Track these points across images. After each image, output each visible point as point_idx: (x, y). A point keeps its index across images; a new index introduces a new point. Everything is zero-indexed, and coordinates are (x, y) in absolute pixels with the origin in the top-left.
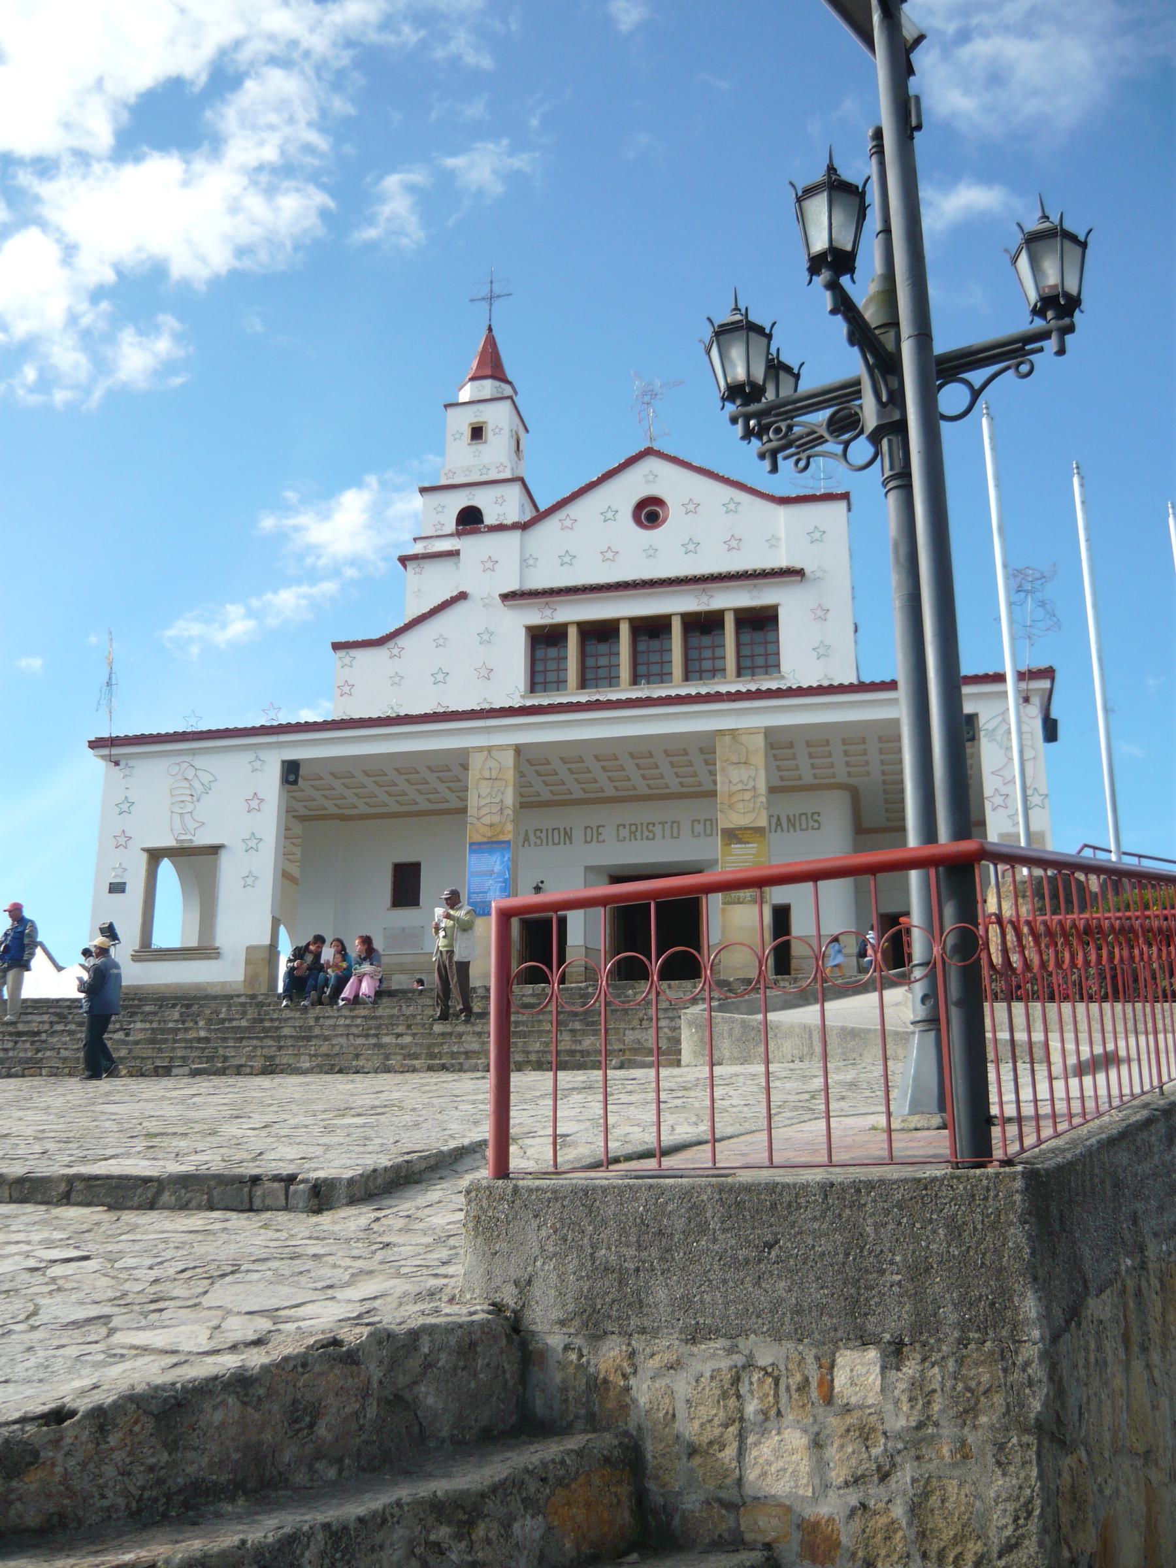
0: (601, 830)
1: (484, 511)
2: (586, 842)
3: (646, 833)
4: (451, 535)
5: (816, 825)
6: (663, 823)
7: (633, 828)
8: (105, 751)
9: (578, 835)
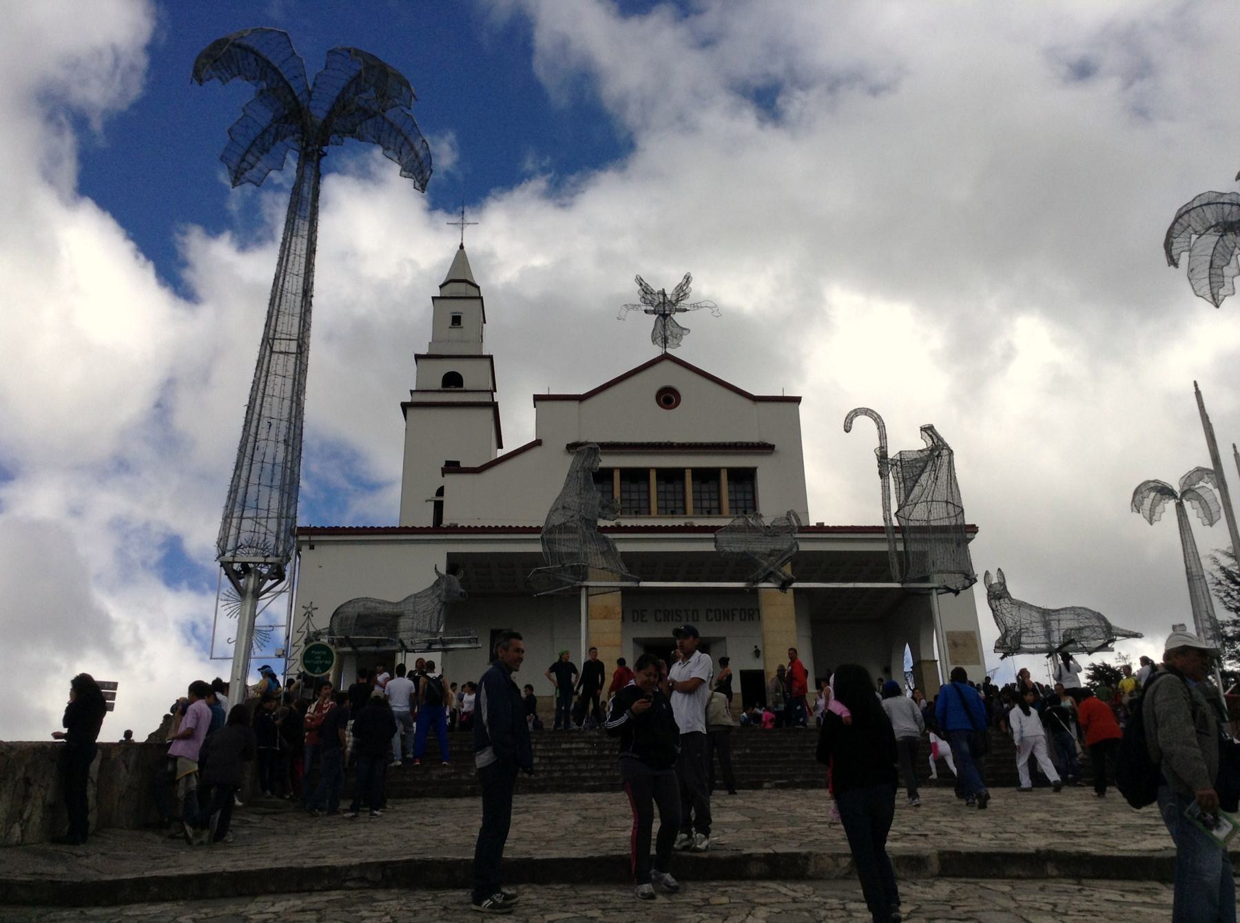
3: (675, 617)
4: (438, 391)
7: (667, 613)
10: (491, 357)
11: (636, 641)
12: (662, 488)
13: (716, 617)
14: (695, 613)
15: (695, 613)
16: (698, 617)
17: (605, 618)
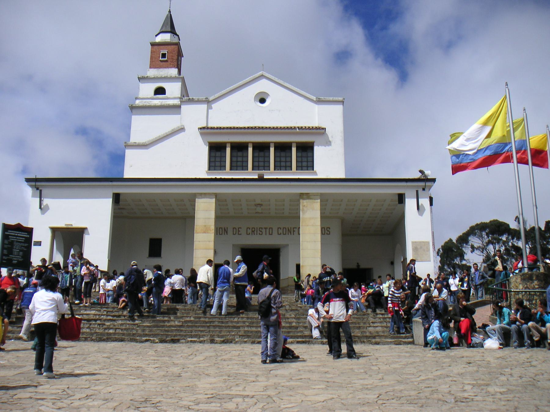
0: (240, 229)
2: (233, 234)
3: (258, 232)
5: (328, 233)
6: (266, 228)
8: (33, 184)
9: (230, 231)
13: (283, 232)
14: (271, 230)
15: (271, 230)
16: (272, 232)
17: (205, 232)
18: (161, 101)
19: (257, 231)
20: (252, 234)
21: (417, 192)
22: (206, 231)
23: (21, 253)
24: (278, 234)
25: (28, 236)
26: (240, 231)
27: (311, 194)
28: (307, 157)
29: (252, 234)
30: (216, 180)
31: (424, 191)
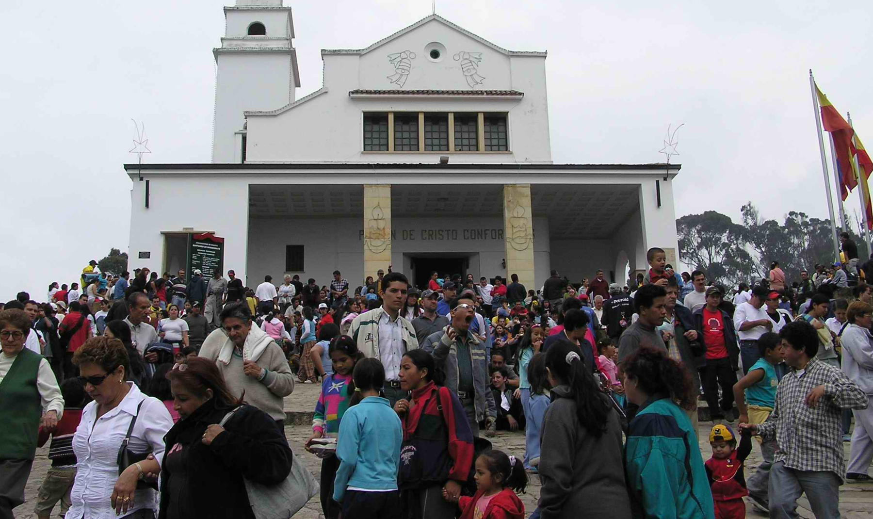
1: (266, 26)
2: (404, 239)
3: (438, 236)
4: (243, 39)
7: (431, 233)
10: (289, 10)
11: (403, 253)
12: (429, 128)
13: (471, 236)
15: (454, 232)
18: (259, 43)
19: (436, 234)
20: (429, 239)
21: (658, 182)
22: (379, 234)
23: (212, 271)
24: (465, 239)
25: (219, 249)
26: (412, 235)
27: (518, 186)
28: (498, 133)
29: (429, 239)
30: (369, 166)
31: (665, 181)
